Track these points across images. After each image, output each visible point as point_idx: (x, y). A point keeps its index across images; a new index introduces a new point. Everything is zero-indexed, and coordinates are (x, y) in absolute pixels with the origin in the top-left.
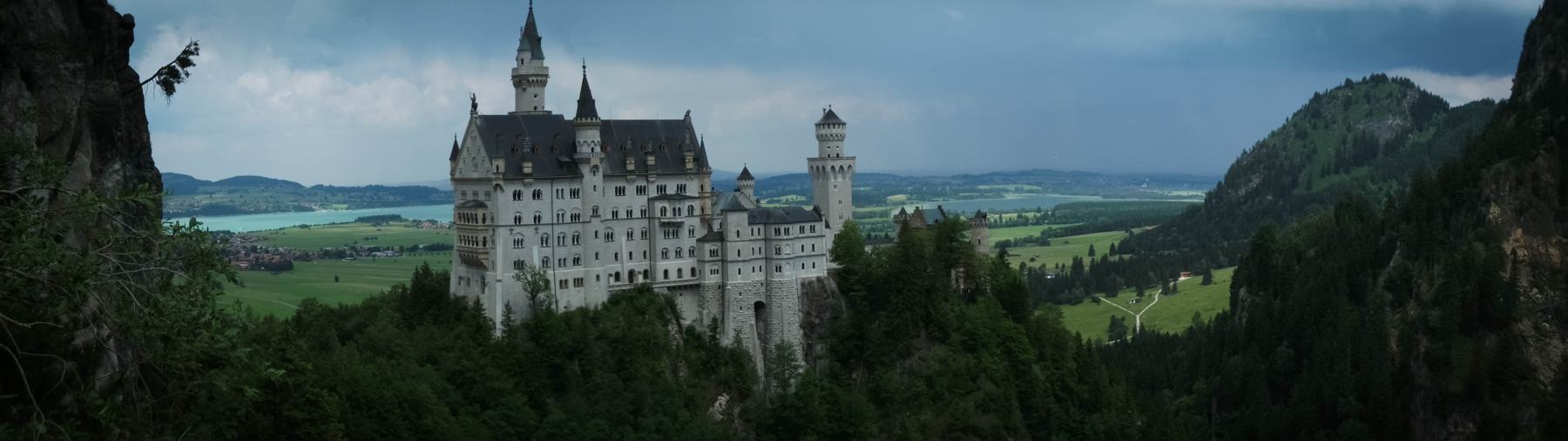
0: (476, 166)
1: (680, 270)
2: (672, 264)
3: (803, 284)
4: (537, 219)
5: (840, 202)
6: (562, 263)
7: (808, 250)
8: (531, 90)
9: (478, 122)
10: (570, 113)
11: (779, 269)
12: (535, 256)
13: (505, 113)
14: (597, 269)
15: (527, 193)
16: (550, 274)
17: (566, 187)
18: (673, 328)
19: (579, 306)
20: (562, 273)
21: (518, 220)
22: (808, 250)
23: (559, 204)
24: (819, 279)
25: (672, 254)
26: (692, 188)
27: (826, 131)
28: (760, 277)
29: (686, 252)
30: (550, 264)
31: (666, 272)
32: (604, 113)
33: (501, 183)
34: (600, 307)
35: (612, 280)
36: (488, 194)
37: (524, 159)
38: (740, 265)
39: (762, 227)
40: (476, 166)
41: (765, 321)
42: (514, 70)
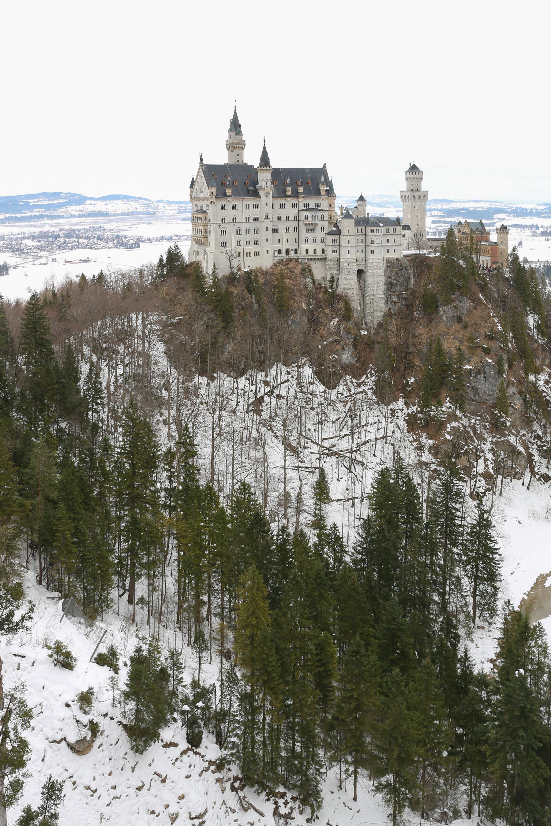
0: (202, 191)
1: (315, 250)
2: (311, 247)
3: (387, 261)
4: (234, 220)
5: (418, 216)
6: (248, 243)
7: (391, 242)
8: (236, 152)
9: (204, 168)
10: (256, 163)
11: (372, 252)
12: (232, 238)
13: (222, 163)
14: (267, 246)
15: (229, 206)
16: (240, 249)
17: (251, 202)
18: (309, 281)
19: (257, 266)
20: (248, 249)
21: (223, 221)
22: (391, 242)
23: (247, 212)
24: (397, 259)
25: (310, 241)
26: (324, 205)
27: (410, 176)
28: (361, 255)
29: (319, 240)
30: (241, 244)
31: (307, 251)
32: (275, 164)
33: (214, 200)
34: (269, 267)
35: (276, 253)
36: (207, 206)
37: (228, 187)
38: (350, 249)
39: (363, 228)
40: (202, 191)
41: (365, 280)
42: (227, 141)
